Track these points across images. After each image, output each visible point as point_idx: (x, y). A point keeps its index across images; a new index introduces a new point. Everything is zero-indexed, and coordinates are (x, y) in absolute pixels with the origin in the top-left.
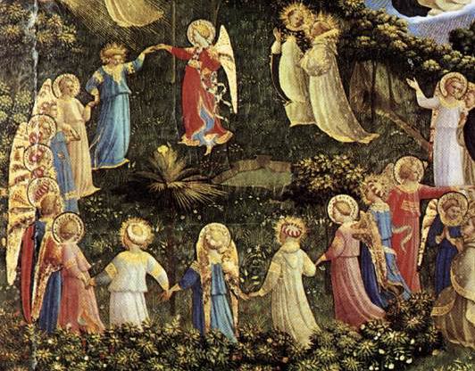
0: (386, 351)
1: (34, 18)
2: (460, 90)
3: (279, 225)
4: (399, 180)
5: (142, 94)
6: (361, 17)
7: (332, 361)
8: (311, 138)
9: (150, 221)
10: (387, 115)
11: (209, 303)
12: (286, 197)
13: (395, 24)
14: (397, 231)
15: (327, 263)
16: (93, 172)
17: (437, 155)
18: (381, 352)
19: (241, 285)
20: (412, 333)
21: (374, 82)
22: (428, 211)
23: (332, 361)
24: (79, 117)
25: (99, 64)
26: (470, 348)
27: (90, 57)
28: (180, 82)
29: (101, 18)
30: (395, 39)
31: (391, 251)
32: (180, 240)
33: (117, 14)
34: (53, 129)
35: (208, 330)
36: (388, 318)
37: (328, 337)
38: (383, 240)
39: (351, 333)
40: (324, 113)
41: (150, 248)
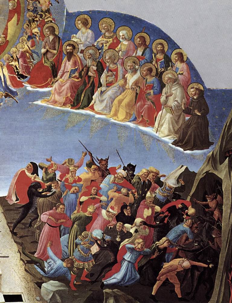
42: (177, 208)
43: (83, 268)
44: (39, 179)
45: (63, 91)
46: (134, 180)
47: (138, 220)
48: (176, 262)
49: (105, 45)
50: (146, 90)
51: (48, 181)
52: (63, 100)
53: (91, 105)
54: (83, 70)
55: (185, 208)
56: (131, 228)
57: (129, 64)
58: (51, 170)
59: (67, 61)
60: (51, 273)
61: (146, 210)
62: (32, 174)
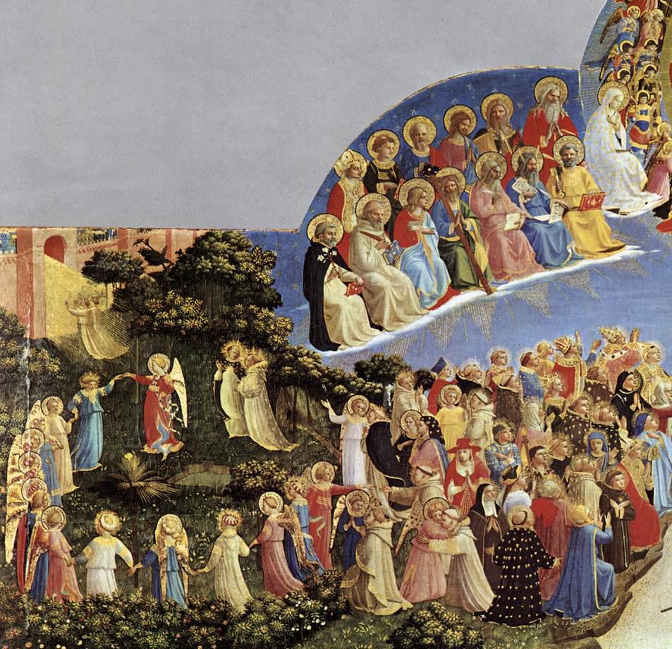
0: (305, 615)
1: (27, 352)
2: (364, 409)
3: (220, 516)
4: (315, 480)
5: (112, 412)
6: (285, 351)
7: (262, 624)
8: (246, 447)
9: (118, 513)
10: (306, 429)
11: (165, 577)
12: (225, 493)
13: (312, 357)
14: (314, 521)
15: (258, 546)
16: (74, 474)
17: (345, 460)
18: (301, 616)
19: (190, 564)
20: (326, 601)
21: (295, 402)
22: (338, 505)
23: (262, 624)
24: (62, 431)
25: (78, 389)
26: (371, 613)
27: (71, 382)
28: (142, 403)
29: (80, 352)
30: (312, 369)
31: (309, 537)
32: (143, 528)
33: (93, 349)
34: (42, 440)
35: (164, 599)
36: (306, 589)
37: (259, 604)
38: (302, 528)
39: (277, 601)
40: (256, 427)
41: (119, 534)
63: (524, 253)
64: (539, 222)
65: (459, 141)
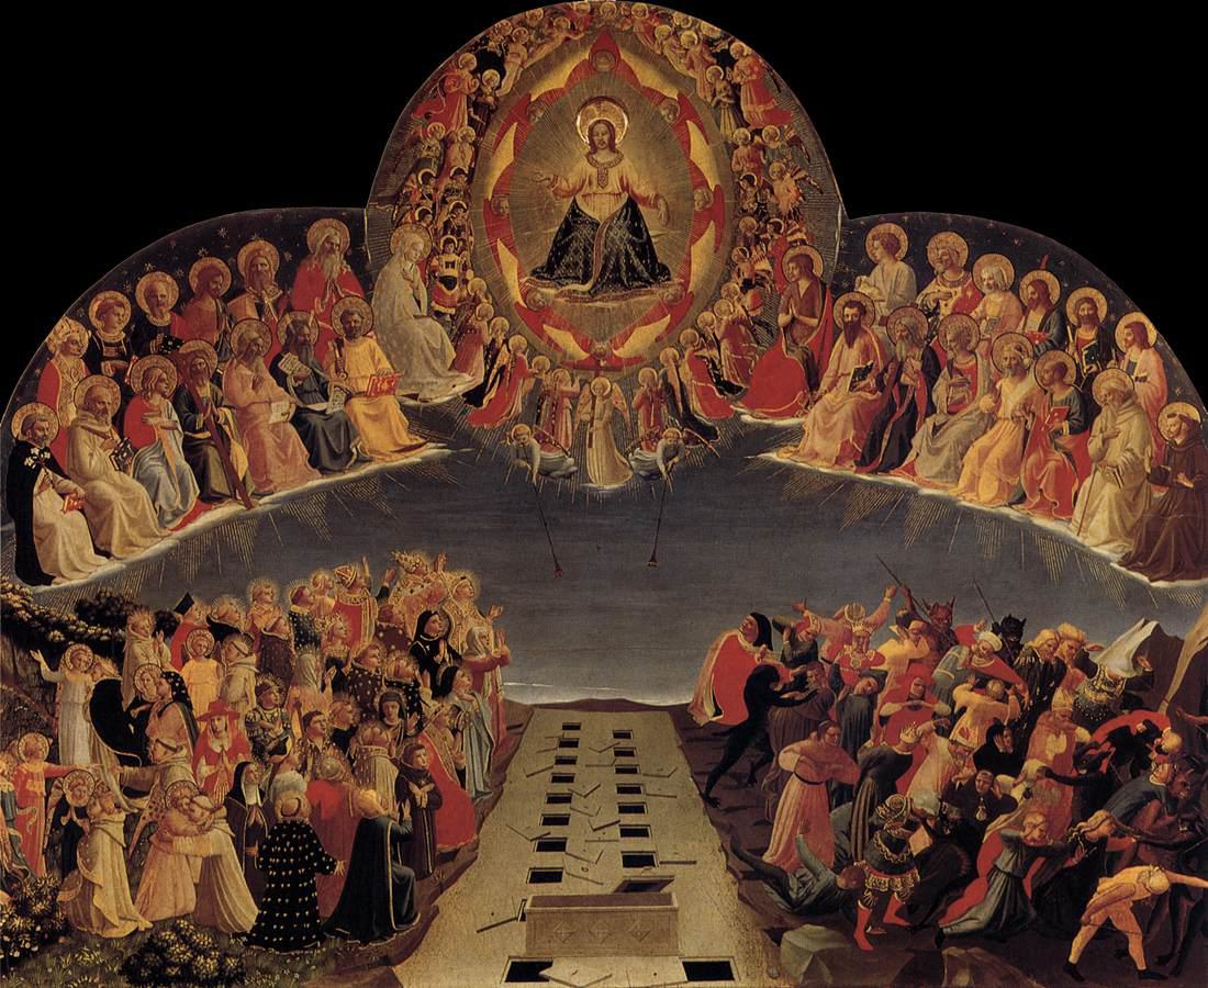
42: (1134, 733)
43: (890, 891)
44: (773, 659)
45: (835, 424)
46: (1021, 660)
47: (1032, 766)
48: (1129, 877)
49: (942, 303)
50: (1051, 421)
51: (796, 662)
52: (835, 448)
53: (906, 462)
54: (886, 370)
55: (1153, 732)
56: (1015, 785)
57: (1006, 354)
58: (804, 633)
59: (846, 346)
60: (806, 902)
61: (1052, 737)
62: (757, 644)
63: (294, 453)
64: (314, 412)
65: (210, 305)
